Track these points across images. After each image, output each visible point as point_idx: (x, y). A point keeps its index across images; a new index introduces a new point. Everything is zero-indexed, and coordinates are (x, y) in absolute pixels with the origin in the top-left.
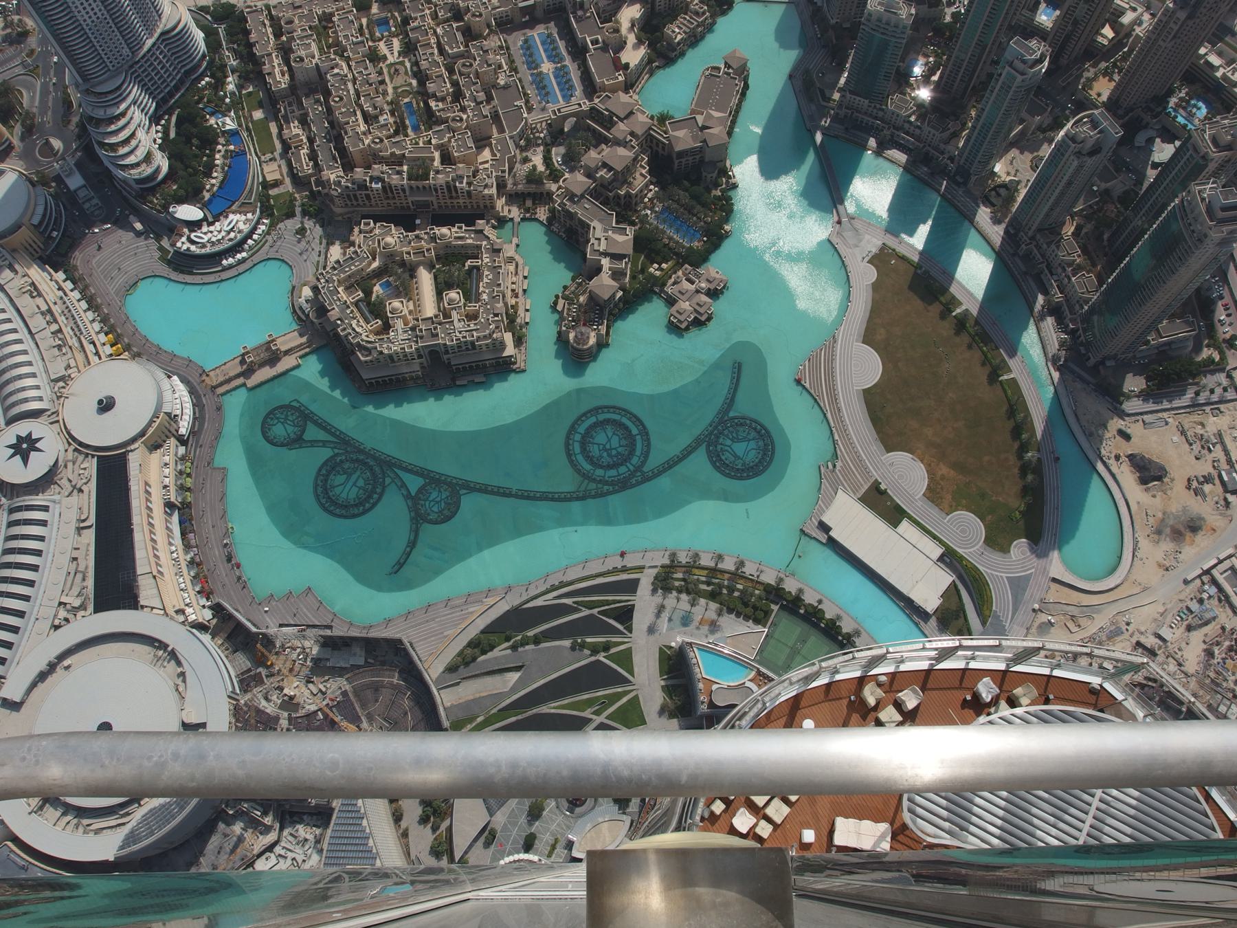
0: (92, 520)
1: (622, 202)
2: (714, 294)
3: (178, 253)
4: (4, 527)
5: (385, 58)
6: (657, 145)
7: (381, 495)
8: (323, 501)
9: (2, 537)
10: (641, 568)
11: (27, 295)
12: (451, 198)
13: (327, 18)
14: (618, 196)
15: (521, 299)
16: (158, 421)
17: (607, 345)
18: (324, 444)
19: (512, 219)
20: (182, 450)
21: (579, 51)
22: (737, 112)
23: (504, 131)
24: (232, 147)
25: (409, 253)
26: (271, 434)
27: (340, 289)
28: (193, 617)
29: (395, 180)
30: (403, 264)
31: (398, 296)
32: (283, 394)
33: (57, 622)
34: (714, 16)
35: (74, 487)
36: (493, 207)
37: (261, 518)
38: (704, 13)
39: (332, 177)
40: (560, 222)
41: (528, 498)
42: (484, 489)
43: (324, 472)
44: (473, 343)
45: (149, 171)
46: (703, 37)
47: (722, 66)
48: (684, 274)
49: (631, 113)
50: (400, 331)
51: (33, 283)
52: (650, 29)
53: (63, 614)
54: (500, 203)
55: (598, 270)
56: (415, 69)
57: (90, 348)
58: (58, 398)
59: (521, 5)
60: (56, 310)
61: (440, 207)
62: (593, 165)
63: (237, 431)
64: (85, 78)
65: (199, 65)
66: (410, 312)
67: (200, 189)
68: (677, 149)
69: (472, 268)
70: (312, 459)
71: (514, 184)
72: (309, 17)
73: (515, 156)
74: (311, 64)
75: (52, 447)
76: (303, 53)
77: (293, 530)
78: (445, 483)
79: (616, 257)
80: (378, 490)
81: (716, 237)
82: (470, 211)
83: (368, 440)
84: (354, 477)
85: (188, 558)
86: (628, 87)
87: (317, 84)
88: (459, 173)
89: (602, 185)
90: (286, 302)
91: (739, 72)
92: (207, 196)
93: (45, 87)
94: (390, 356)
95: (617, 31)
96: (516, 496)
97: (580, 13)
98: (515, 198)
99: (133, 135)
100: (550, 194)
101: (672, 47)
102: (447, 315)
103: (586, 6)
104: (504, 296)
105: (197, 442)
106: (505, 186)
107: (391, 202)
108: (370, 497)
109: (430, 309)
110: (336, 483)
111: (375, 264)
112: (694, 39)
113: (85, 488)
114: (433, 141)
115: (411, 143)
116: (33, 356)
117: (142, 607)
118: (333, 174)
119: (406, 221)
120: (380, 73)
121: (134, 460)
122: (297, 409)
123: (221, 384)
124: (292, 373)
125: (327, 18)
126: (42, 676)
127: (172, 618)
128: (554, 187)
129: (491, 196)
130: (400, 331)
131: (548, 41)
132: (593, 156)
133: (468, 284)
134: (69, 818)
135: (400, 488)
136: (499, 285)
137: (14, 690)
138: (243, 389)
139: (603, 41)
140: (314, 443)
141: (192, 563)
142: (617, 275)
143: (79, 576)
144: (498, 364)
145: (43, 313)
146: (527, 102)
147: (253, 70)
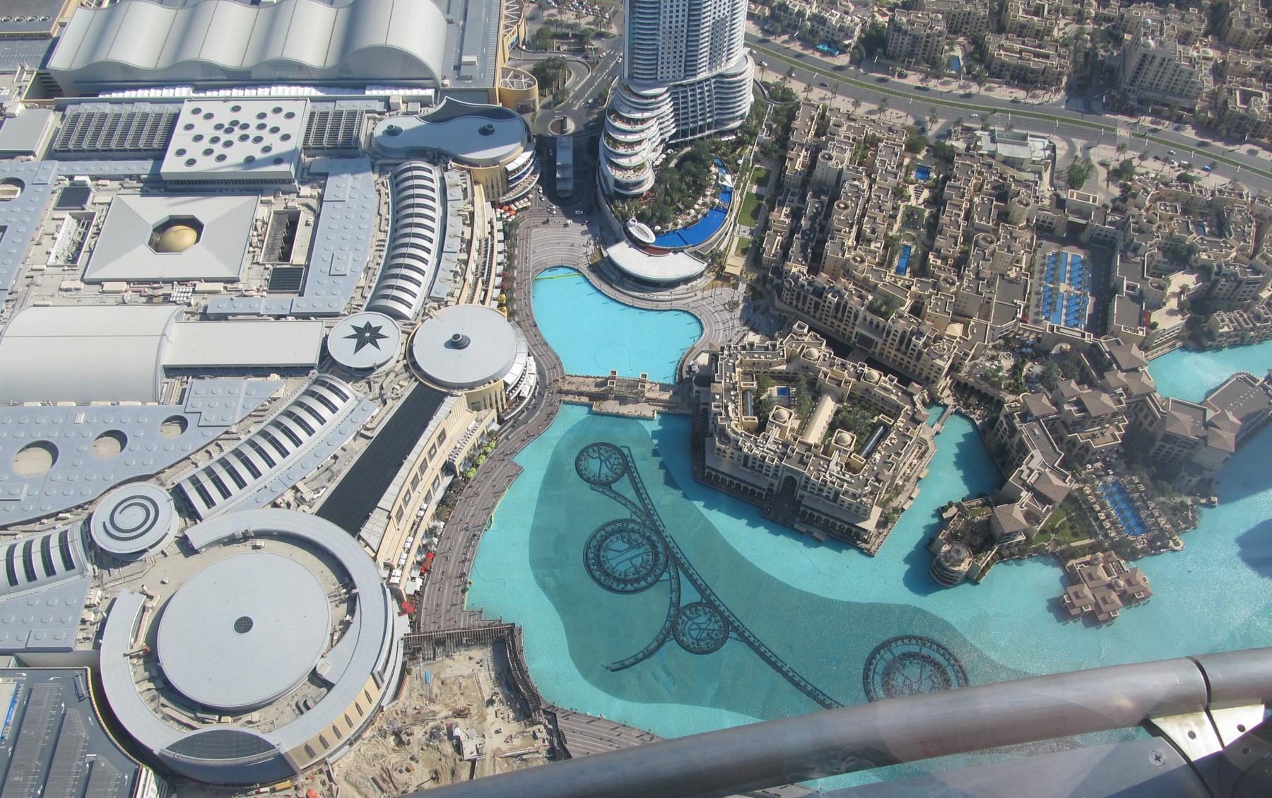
0: (375, 434)
1: (1076, 451)
2: (1128, 599)
4: (300, 392)
5: (909, 199)
6: (1146, 417)
9: (293, 399)
12: (898, 350)
13: (873, 142)
14: (1073, 442)
15: (908, 486)
17: (976, 582)
18: (626, 502)
20: (496, 427)
23: (987, 318)
24: (717, 201)
25: (826, 375)
27: (737, 370)
28: (394, 580)
31: (789, 407)
32: (621, 436)
33: (279, 501)
35: (381, 395)
37: (522, 535)
39: (794, 270)
41: (797, 685)
42: (756, 647)
44: (837, 493)
46: (1250, 344)
51: (472, 214)
54: (944, 382)
55: (1013, 500)
57: (479, 294)
58: (425, 314)
59: (1072, 218)
60: (475, 244)
61: (881, 354)
63: (555, 442)
64: (631, 76)
66: (792, 430)
67: (662, 220)
68: (1172, 429)
70: (605, 510)
71: (969, 373)
75: (390, 349)
76: (834, 154)
77: (545, 562)
78: (721, 614)
79: (1041, 498)
80: (650, 579)
84: (635, 552)
85: (432, 524)
86: (1144, 347)
88: (923, 328)
89: (1063, 422)
90: (677, 356)
93: (592, 80)
94: (747, 457)
95: (1162, 288)
96: (785, 674)
97: (1129, 254)
99: (639, 142)
100: (1000, 404)
101: (1211, 335)
102: (827, 451)
103: (1139, 252)
105: (516, 416)
106: (958, 370)
107: (836, 323)
108: (637, 581)
109: (815, 435)
111: (783, 367)
112: (1240, 340)
114: (913, 288)
116: (429, 269)
117: (360, 538)
118: (796, 268)
119: (841, 348)
120: (895, 208)
123: (567, 393)
124: (642, 422)
126: (232, 540)
129: (940, 369)
130: (771, 440)
132: (1072, 387)
133: (868, 437)
134: (151, 685)
135: (672, 591)
136: (899, 454)
137: (197, 536)
138: (586, 409)
139: (1141, 291)
140: (618, 497)
141: (431, 532)
142: (1031, 516)
143: (328, 474)
144: (849, 531)
145: (462, 240)
146: (1027, 307)
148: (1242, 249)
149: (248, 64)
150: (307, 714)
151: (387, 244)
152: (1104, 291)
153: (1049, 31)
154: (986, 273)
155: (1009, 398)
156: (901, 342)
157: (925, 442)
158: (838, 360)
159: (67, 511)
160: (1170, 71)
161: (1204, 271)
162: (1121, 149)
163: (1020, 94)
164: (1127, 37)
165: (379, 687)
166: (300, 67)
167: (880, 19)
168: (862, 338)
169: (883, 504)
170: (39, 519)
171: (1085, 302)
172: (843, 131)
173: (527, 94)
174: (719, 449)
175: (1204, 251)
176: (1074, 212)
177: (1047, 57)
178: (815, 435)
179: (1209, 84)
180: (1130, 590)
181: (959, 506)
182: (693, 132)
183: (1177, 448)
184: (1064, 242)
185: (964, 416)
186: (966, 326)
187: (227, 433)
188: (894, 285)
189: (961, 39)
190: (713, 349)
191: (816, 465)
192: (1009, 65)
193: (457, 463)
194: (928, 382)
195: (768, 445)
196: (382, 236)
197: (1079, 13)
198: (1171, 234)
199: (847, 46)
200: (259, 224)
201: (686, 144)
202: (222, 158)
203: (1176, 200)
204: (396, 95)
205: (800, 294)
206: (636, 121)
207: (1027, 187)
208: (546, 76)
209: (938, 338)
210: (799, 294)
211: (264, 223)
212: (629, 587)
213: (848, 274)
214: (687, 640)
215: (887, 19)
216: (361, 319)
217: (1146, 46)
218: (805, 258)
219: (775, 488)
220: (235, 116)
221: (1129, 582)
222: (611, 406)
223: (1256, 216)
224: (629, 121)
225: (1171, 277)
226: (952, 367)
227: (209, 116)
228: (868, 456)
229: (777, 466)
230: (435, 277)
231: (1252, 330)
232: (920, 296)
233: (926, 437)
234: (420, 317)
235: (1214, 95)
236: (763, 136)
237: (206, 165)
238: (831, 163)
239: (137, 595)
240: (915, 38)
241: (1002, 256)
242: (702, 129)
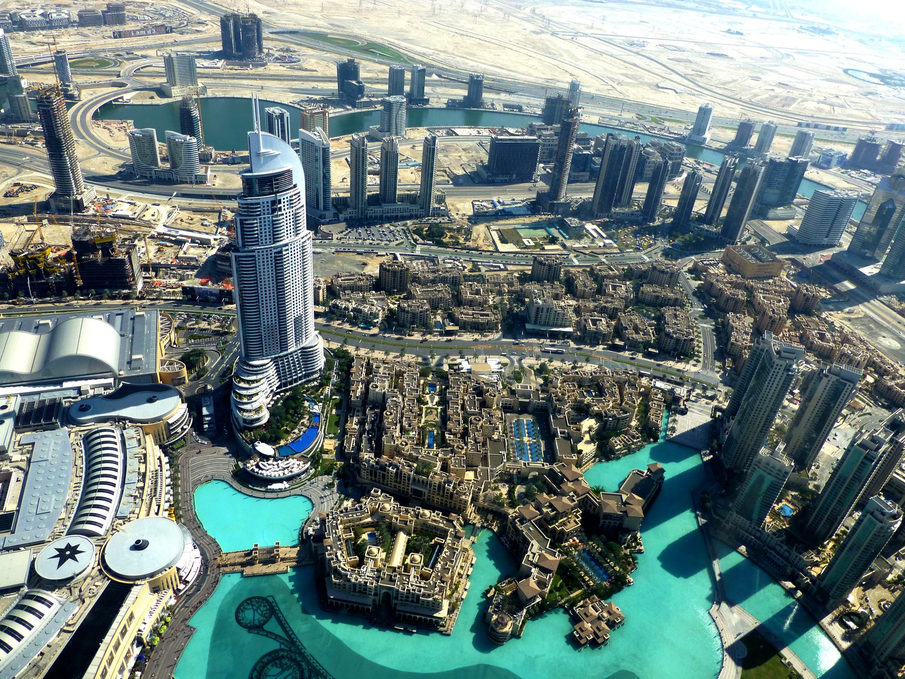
2: (612, 625)
3: (244, 470)
4: (11, 608)
5: (427, 403)
6: (590, 506)
13: (400, 374)
14: (554, 529)
15: (463, 580)
17: (518, 637)
18: (276, 637)
19: (474, 524)
25: (397, 519)
27: (340, 527)
31: (376, 545)
32: (265, 588)
38: (638, 438)
40: (508, 537)
44: (418, 596)
45: (256, 416)
50: (369, 569)
51: (145, 455)
54: (470, 509)
55: (528, 575)
57: (154, 508)
58: (113, 529)
60: (149, 475)
61: (429, 499)
63: (218, 604)
68: (606, 510)
71: (484, 501)
72: (391, 369)
76: (379, 384)
81: (619, 583)
82: (449, 506)
83: (309, 646)
84: (287, 673)
86: (579, 465)
87: (380, 404)
88: (450, 478)
89: (545, 520)
90: (298, 525)
94: (355, 585)
95: (579, 430)
98: (480, 510)
99: (257, 394)
100: (506, 515)
101: (612, 451)
102: (407, 568)
107: (398, 485)
109: (396, 561)
110: (271, 673)
111: (369, 520)
113: (87, 601)
116: (115, 498)
119: (403, 499)
120: (421, 409)
122: (270, 603)
125: (400, 374)
129: (466, 502)
133: (432, 554)
136: (452, 562)
138: (239, 575)
140: (269, 634)
142: (541, 584)
143: (35, 669)
145: (139, 473)
146: (508, 454)
147: (344, 387)
151: (82, 485)
152: (549, 436)
153: (486, 302)
154: (481, 439)
155: (511, 511)
158: (403, 508)
161: (598, 416)
162: (538, 358)
163: (477, 336)
164: (527, 300)
166: (12, 374)
167: (392, 306)
168: (415, 491)
169: (449, 597)
171: (540, 446)
172: (381, 370)
174: (335, 584)
176: (522, 396)
177: (487, 315)
178: (396, 561)
179: (575, 318)
180: (611, 618)
182: (291, 383)
184: (520, 413)
185: (487, 527)
186: (476, 472)
188: (428, 456)
191: (401, 580)
193: (144, 637)
201: (286, 391)
203: (573, 381)
205: (372, 471)
206: (253, 382)
207: (492, 386)
208: (191, 360)
209: (461, 483)
210: (371, 471)
213: (399, 454)
217: (537, 303)
218: (371, 447)
221: (609, 613)
222: (258, 569)
224: (248, 382)
226: (473, 500)
228: (433, 567)
229: (376, 587)
230: (120, 502)
232: (445, 459)
233: (467, 546)
234: (110, 532)
235: (578, 323)
236: (334, 379)
238: (377, 390)
240: (414, 315)
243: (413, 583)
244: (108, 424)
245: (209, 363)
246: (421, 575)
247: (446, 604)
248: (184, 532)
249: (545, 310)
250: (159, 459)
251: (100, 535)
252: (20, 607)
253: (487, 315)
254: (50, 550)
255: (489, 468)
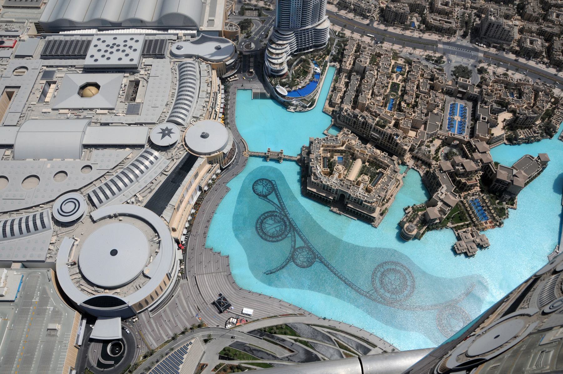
0: (169, 173)
1: (460, 186)
2: (481, 247)
6: (489, 172)
7: (283, 239)
8: (258, 226)
9: (135, 159)
10: (374, 346)
11: (206, 84)
12: (388, 142)
13: (379, 55)
16: (218, 153)
19: (408, 166)
20: (219, 171)
21: (475, 118)
22: (532, 179)
26: (256, 187)
29: (370, 121)
30: (353, 154)
33: (129, 201)
34: (543, 137)
36: (403, 156)
38: (538, 133)
39: (345, 108)
42: (327, 265)
43: (266, 215)
44: (362, 201)
45: (278, 69)
46: (532, 142)
47: (536, 157)
48: (471, 230)
49: (485, 152)
50: (335, 178)
52: (511, 126)
53: (133, 199)
54: (408, 156)
55: (435, 205)
56: (403, 89)
60: (212, 95)
62: (457, 162)
63: (244, 178)
64: (278, 26)
65: (321, 45)
67: (291, 87)
69: (380, 172)
70: (264, 207)
71: (417, 153)
72: (373, 51)
73: (424, 141)
74: (363, 65)
76: (363, 60)
78: (313, 252)
79: (445, 203)
83: (292, 214)
86: (489, 143)
88: (399, 133)
91: (542, 163)
92: (293, 89)
93: (262, 28)
94: (324, 185)
95: (496, 119)
97: (483, 105)
98: (415, 158)
99: (282, 53)
101: (516, 139)
102: (358, 184)
103: (487, 104)
104: (386, 192)
107: (363, 130)
108: (278, 237)
112: (528, 141)
114: (395, 116)
115: (386, 112)
118: (347, 107)
119: (364, 140)
120: (388, 83)
121: (200, 161)
122: (273, 185)
126: (110, 217)
127: (169, 229)
128: (434, 162)
129: (405, 150)
130: (335, 178)
131: (463, 109)
132: (459, 159)
133: (375, 178)
137: (96, 215)
140: (270, 201)
142: (442, 211)
143: (149, 190)
146: (441, 125)
147: (339, 58)
148: (529, 103)
149: (120, 20)
150: (140, 290)
153: (451, 12)
156: (389, 139)
157: (399, 180)
158: (363, 146)
159: (43, 204)
160: (500, 30)
161: (513, 112)
164: (483, 16)
165: (169, 280)
166: (142, 21)
167: (382, 5)
170: (31, 207)
173: (236, 32)
174: (313, 182)
175: (513, 104)
177: (450, 23)
180: (481, 244)
181: (413, 207)
182: (304, 49)
183: (501, 185)
187: (108, 172)
189: (416, 15)
190: (311, 140)
192: (435, 26)
194: (401, 154)
195: (333, 181)
196: (173, 91)
197: (464, 5)
198: (500, 96)
199: (368, 16)
200: (123, 86)
202: (108, 58)
203: (502, 83)
204: (181, 32)
208: (245, 25)
211: (125, 86)
212: (274, 239)
214: (298, 261)
215: (385, 5)
216: (164, 125)
217: (491, 19)
219: (336, 199)
220: (115, 41)
223: (534, 90)
225: (500, 114)
227: (104, 41)
229: (337, 190)
231: (532, 137)
232: (397, 120)
237: (102, 62)
239: (71, 239)
240: (396, 14)
241: (432, 104)
242: (308, 49)
243: (359, 193)
244: (192, 59)
245: (254, 29)
246: (366, 189)
247: (378, 210)
248: (229, 133)
249: (495, 26)
250: (219, 86)
251: (183, 125)
252: (142, 156)
253: (450, 23)
254: (158, 129)
255: (426, 132)
